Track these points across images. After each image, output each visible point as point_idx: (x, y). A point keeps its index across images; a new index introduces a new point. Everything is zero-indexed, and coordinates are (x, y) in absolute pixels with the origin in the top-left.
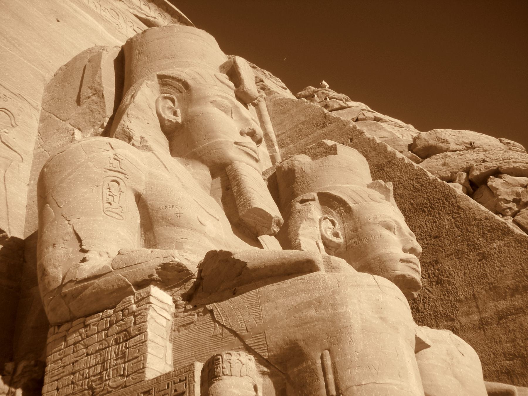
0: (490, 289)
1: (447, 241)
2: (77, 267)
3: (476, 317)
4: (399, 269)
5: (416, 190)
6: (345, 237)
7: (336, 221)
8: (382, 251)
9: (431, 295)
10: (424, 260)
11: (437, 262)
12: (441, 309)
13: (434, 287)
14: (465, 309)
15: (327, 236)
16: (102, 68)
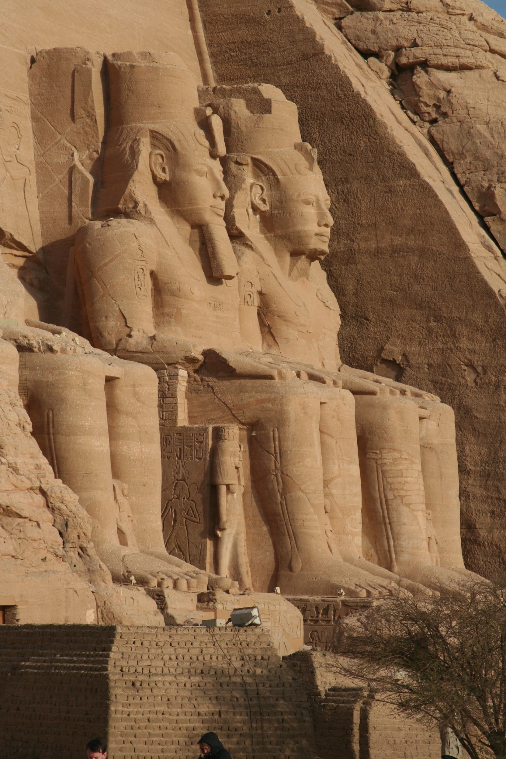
0: (390, 222)
1: (359, 162)
2: (127, 341)
3: (373, 245)
4: (312, 243)
5: (339, 98)
6: (271, 205)
7: (265, 188)
8: (300, 228)
9: (337, 212)
10: (336, 175)
11: (347, 181)
12: (344, 227)
13: (341, 204)
14: (365, 234)
15: (256, 203)
16: (93, 89)
